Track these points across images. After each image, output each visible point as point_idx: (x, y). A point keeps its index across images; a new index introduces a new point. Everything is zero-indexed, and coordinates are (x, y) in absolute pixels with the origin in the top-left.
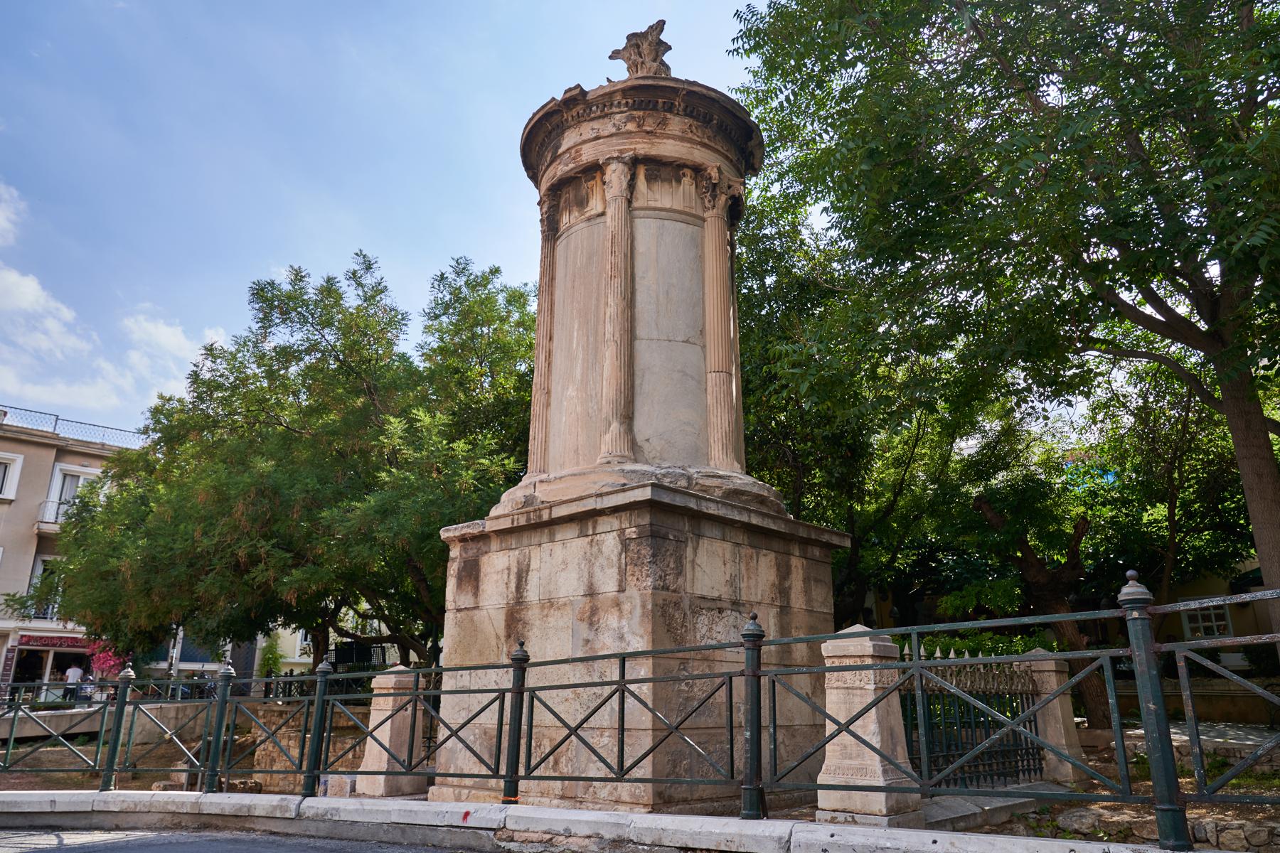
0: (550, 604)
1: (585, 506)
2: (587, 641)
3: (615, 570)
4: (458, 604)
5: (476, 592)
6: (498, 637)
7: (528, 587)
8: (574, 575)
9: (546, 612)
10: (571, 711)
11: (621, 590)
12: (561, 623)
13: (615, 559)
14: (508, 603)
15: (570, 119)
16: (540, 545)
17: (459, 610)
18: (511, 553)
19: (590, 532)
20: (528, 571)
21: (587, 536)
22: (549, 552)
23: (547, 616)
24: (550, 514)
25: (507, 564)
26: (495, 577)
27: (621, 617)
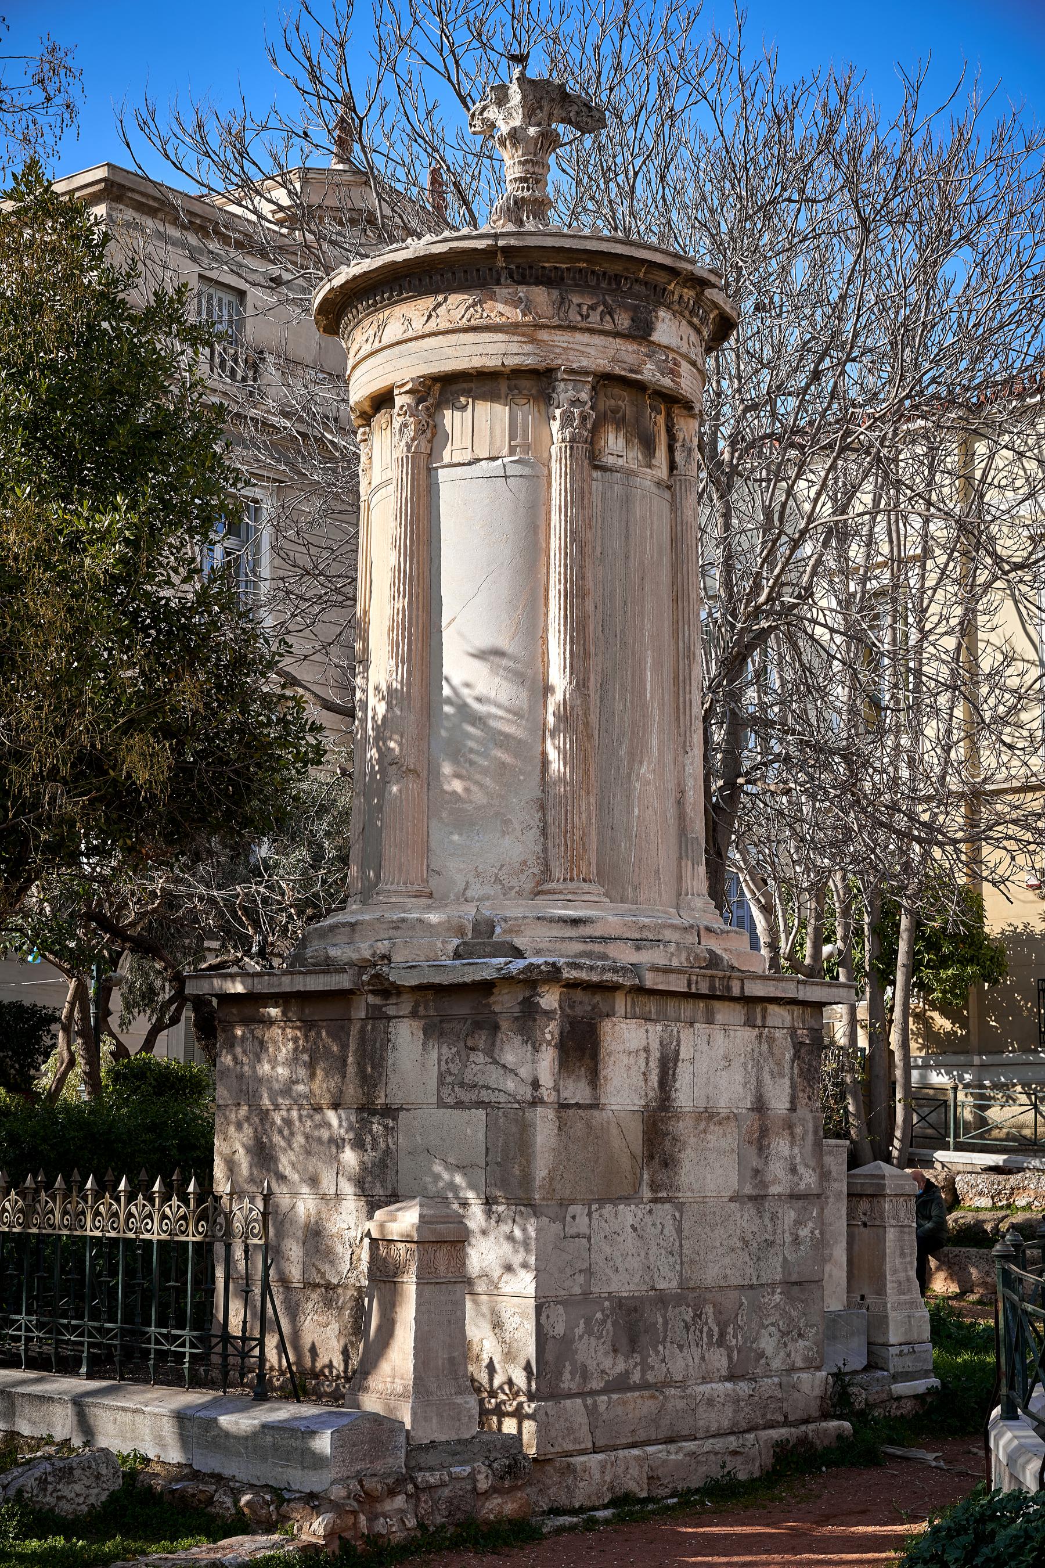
0: (708, 1115)
1: (784, 991)
2: (757, 1172)
3: (787, 1081)
4: (564, 1095)
5: (594, 1078)
6: (633, 1156)
7: (677, 1085)
8: (739, 1077)
9: (703, 1124)
10: (739, 1264)
11: (793, 1109)
12: (724, 1144)
13: (787, 1066)
14: (645, 1107)
16: (691, 1024)
17: (563, 1106)
18: (650, 1026)
19: (759, 1023)
20: (676, 1060)
21: (754, 1026)
22: (705, 1038)
23: (705, 1131)
24: (742, 988)
25: (644, 1043)
26: (625, 1060)
27: (792, 1144)
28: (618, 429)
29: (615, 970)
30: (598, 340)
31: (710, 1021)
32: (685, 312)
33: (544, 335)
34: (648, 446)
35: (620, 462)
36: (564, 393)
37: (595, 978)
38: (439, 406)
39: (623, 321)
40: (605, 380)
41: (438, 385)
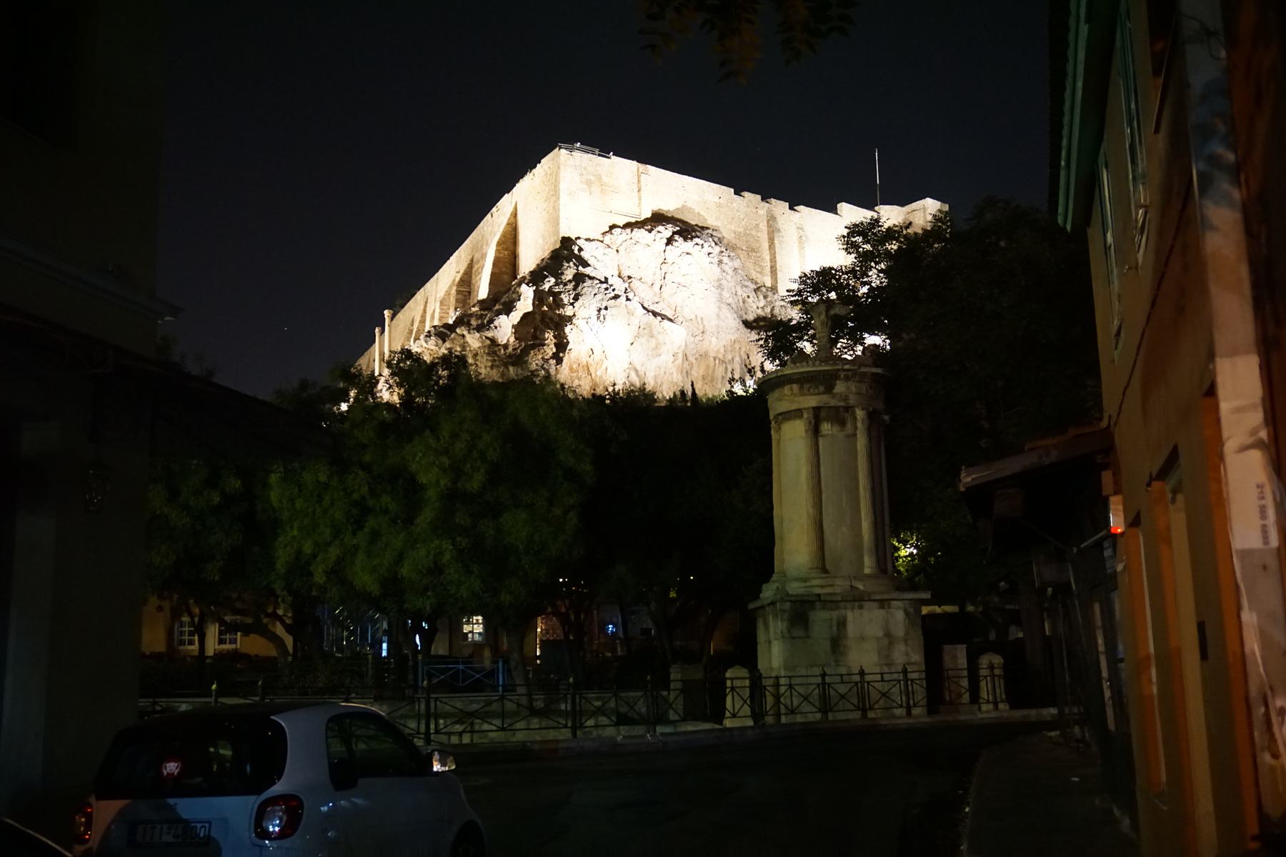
0: (863, 638)
11: (907, 634)
15: (842, 376)
18: (832, 612)
19: (886, 606)
28: (828, 423)
29: (808, 596)
30: (813, 397)
31: (861, 607)
32: (847, 379)
33: (796, 399)
34: (842, 423)
35: (830, 432)
36: (805, 415)
37: (798, 599)
38: (781, 423)
39: (822, 389)
40: (817, 410)
41: (780, 417)
